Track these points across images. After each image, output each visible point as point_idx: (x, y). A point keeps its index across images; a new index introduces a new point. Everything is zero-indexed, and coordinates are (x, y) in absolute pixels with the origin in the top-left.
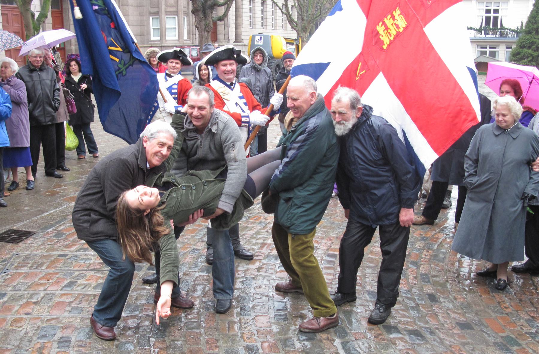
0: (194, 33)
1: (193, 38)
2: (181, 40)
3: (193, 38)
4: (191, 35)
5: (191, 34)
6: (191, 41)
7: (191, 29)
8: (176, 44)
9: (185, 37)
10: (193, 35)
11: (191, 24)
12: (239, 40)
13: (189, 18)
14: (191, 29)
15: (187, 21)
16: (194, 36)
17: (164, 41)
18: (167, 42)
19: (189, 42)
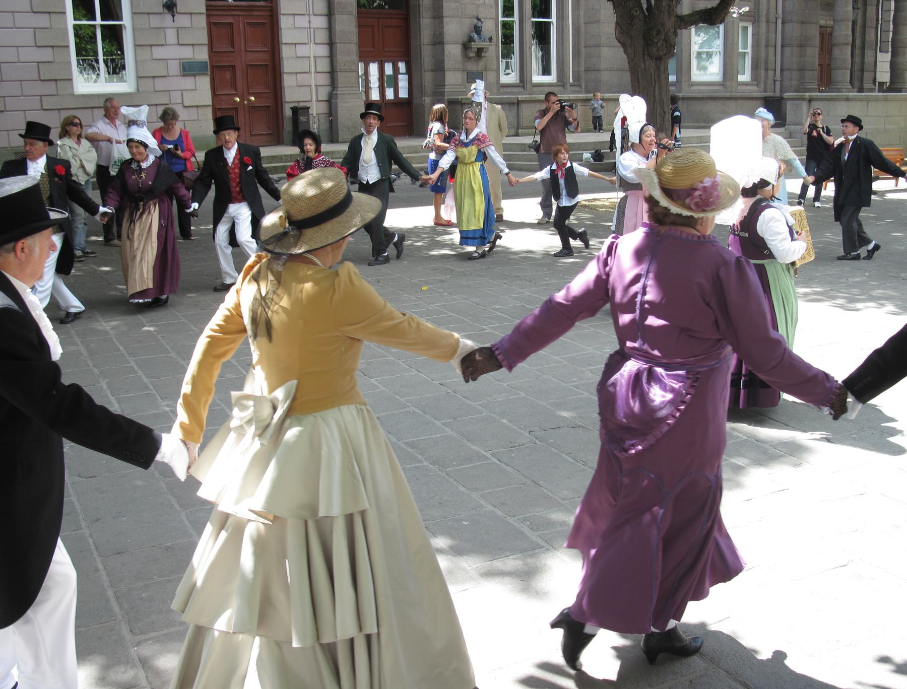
0: (771, 66)
1: (766, 77)
2: (728, 84)
3: (766, 77)
4: (763, 72)
5: (763, 66)
6: (762, 85)
7: (763, 55)
8: (715, 91)
9: (745, 77)
10: (766, 70)
11: (763, 43)
12: (898, 86)
13: (758, 27)
14: (763, 55)
15: (753, 35)
16: (771, 73)
17: (684, 85)
18: (693, 88)
19: (755, 88)
